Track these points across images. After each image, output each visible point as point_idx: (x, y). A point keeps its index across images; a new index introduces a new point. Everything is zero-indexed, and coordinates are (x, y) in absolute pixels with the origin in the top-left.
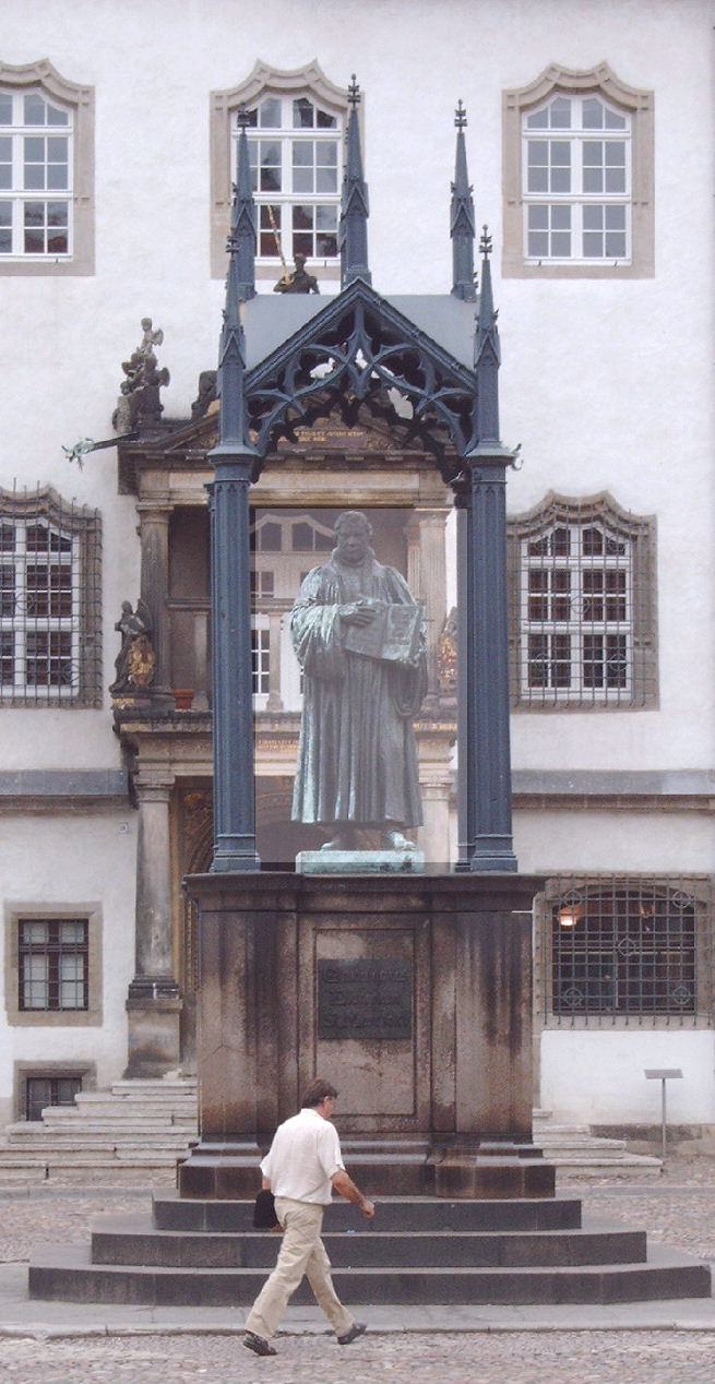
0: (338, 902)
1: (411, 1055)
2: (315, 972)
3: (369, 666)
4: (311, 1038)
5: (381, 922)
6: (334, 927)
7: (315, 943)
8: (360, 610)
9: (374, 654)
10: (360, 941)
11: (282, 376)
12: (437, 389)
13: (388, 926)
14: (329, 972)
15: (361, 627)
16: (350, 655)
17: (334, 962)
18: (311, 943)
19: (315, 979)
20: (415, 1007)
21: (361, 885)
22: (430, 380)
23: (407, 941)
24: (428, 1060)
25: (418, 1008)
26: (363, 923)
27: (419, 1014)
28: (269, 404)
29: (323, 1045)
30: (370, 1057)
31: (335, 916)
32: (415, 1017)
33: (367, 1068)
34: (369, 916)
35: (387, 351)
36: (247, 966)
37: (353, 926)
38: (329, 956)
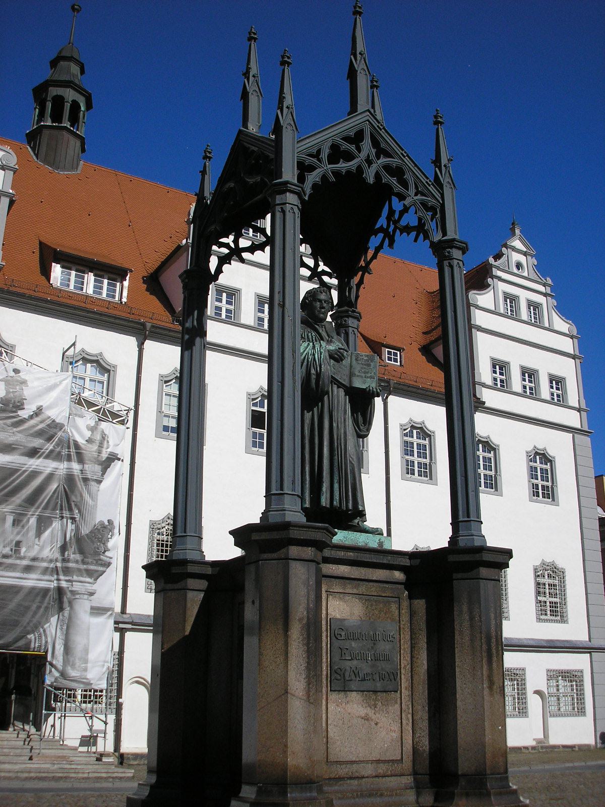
0: (343, 570)
1: (397, 706)
3: (342, 392)
4: (324, 690)
5: (374, 589)
8: (339, 348)
9: (346, 383)
10: (361, 605)
11: (319, 151)
12: (416, 195)
13: (380, 594)
14: (339, 630)
16: (334, 381)
17: (342, 620)
20: (400, 665)
23: (394, 607)
24: (411, 711)
25: (402, 666)
26: (363, 588)
27: (403, 671)
28: (311, 168)
29: (333, 696)
30: (369, 708)
32: (401, 673)
33: (366, 718)
35: (383, 160)
36: (308, 612)
37: (355, 591)
38: (338, 616)
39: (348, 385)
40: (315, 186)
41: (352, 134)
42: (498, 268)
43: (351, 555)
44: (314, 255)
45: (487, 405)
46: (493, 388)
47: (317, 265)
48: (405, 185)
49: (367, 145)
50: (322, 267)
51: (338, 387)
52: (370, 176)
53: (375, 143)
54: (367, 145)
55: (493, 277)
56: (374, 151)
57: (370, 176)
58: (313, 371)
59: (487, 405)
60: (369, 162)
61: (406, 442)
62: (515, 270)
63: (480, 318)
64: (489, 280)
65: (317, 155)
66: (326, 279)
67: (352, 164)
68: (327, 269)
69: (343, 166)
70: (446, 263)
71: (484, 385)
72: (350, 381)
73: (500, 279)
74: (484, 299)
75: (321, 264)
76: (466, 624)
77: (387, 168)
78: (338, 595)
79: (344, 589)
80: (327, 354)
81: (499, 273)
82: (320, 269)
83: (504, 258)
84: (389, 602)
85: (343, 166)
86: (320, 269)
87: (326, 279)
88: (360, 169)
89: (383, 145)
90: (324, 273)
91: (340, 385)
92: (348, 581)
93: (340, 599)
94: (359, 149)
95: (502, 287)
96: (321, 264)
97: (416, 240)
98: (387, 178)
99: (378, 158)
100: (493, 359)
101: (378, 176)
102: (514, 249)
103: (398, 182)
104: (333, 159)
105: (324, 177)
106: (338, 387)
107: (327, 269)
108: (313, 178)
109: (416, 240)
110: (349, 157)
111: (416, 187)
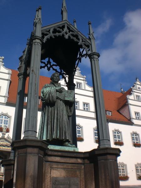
0: (58, 159)
2: (50, 181)
5: (70, 166)
6: (56, 167)
7: (50, 172)
10: (64, 172)
11: (49, 30)
13: (72, 168)
15: (60, 93)
16: (57, 98)
17: (56, 178)
18: (49, 172)
19: (50, 184)
21: (64, 154)
26: (65, 166)
28: (46, 35)
31: (57, 163)
34: (67, 164)
37: (62, 167)
38: (55, 176)
39: (64, 100)
40: (47, 39)
42: (134, 89)
43: (60, 154)
44: (60, 69)
45: (135, 124)
46: (136, 119)
47: (61, 71)
48: (79, 39)
50: (63, 72)
51: (60, 100)
52: (66, 37)
53: (68, 28)
54: (66, 29)
55: (132, 91)
57: (66, 37)
58: (50, 95)
59: (135, 124)
60: (66, 33)
61: (114, 135)
62: (138, 89)
63: (130, 102)
64: (132, 92)
65: (49, 31)
67: (61, 34)
69: (57, 34)
70: (92, 60)
71: (133, 119)
72: (64, 98)
73: (135, 92)
74: (131, 97)
75: (62, 71)
76: (103, 177)
77: (72, 35)
78: (55, 169)
79: (57, 166)
80: (55, 90)
81: (134, 90)
82: (62, 73)
83: (135, 86)
84: (76, 171)
85: (57, 34)
86: (62, 73)
88: (63, 35)
89: (71, 29)
91: (61, 100)
92: (59, 163)
93: (56, 170)
94: (63, 30)
95: (135, 94)
96: (62, 71)
97: (86, 58)
98: (72, 37)
100: (135, 112)
101: (69, 37)
102: (137, 84)
104: (53, 32)
105: (51, 37)
106: (60, 100)
108: (46, 37)
109: (86, 58)
110: (59, 32)
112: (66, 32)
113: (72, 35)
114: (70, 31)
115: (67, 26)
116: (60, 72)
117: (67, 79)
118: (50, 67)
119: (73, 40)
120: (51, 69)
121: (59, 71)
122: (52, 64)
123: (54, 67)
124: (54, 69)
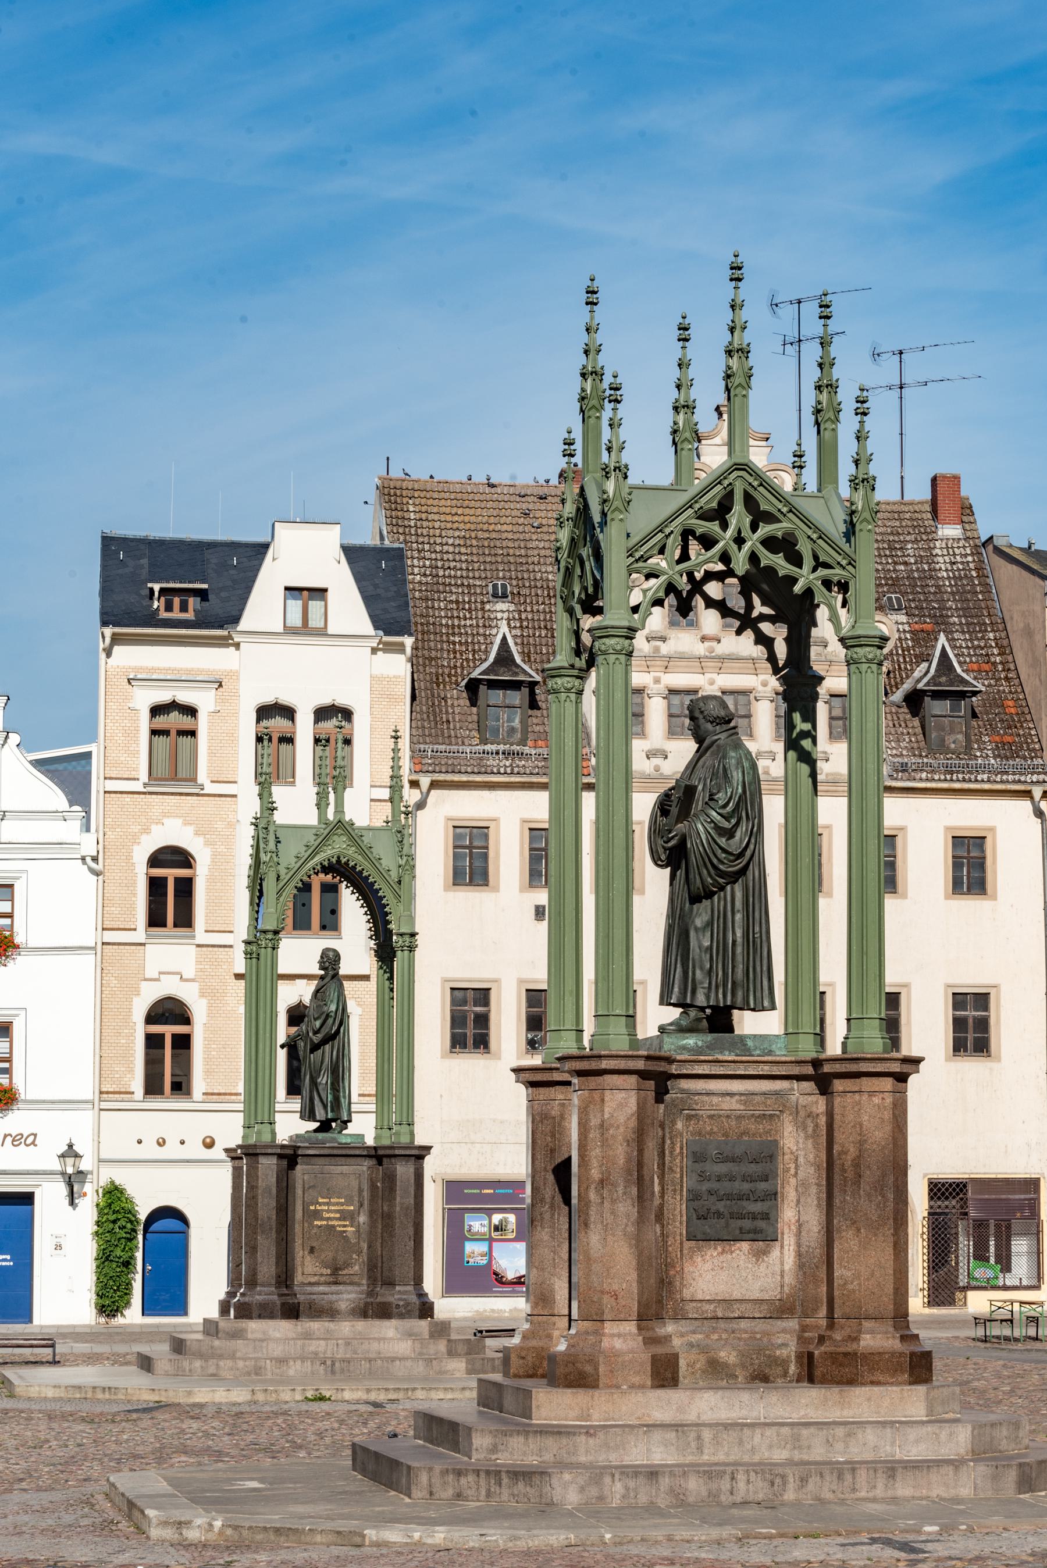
12: (814, 570)
22: (808, 562)
41: (714, 505)
44: (746, 593)
47: (750, 607)
48: (796, 560)
49: (738, 517)
50: (759, 608)
54: (738, 517)
56: (748, 520)
60: (740, 541)
66: (766, 627)
68: (767, 611)
75: (756, 600)
77: (769, 543)
82: (755, 614)
86: (755, 614)
87: (766, 627)
90: (763, 617)
94: (725, 526)
96: (756, 600)
98: (767, 558)
99: (754, 528)
101: (754, 558)
103: (788, 559)
107: (767, 611)
111: (816, 557)
112: (739, 532)
113: (769, 543)
114: (759, 517)
115: (745, 490)
116: (742, 611)
117: (781, 650)
118: (691, 594)
119: (771, 570)
120: (699, 602)
121: (737, 603)
122: (698, 576)
123: (713, 589)
124: (710, 603)
